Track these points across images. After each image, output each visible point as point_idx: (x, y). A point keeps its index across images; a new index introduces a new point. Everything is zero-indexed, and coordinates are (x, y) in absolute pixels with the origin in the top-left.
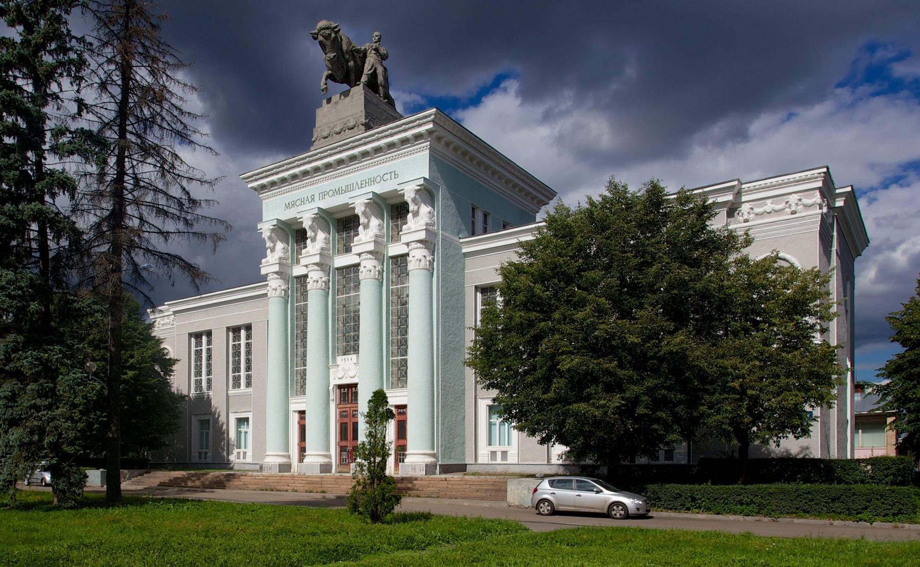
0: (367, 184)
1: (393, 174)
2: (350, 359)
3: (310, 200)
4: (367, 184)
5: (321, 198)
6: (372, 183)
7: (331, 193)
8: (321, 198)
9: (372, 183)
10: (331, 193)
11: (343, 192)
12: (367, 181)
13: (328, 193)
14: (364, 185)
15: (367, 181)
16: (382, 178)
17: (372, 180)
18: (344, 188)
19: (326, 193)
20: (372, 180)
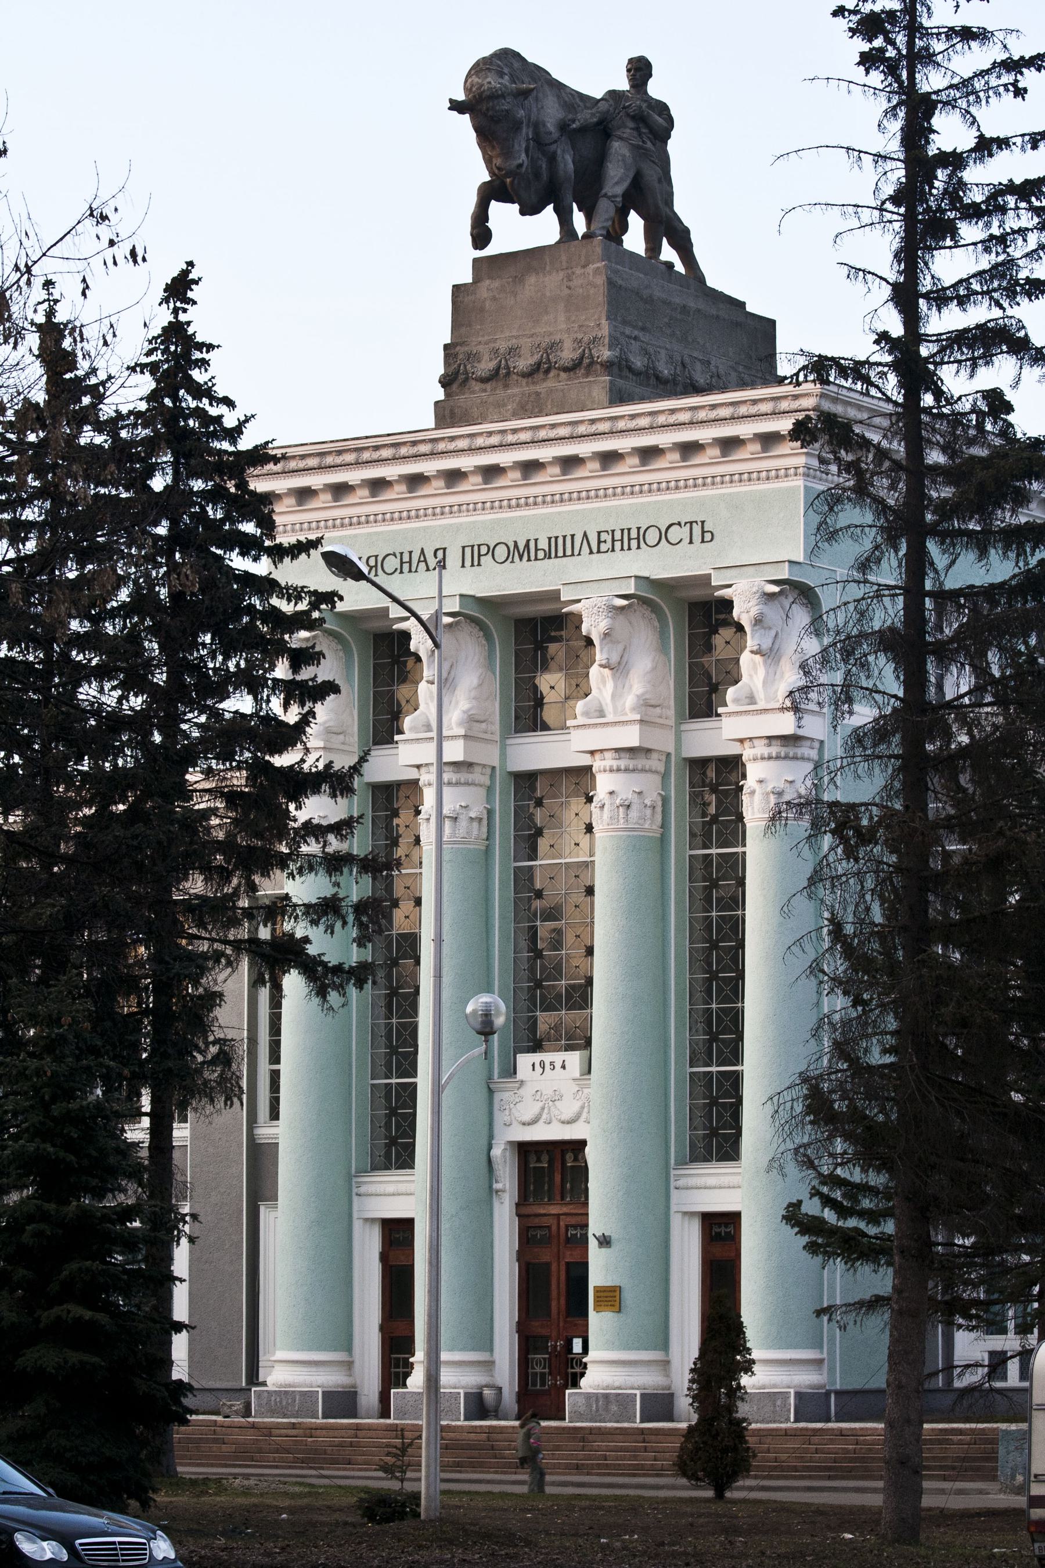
0: (618, 545)
1: (697, 530)
2: (537, 1066)
3: (432, 562)
4: (618, 545)
5: (468, 563)
6: (634, 543)
7: (501, 552)
8: (468, 563)
9: (634, 543)
10: (501, 552)
11: (541, 555)
12: (618, 536)
13: (491, 551)
14: (609, 545)
15: (618, 536)
16: (664, 535)
17: (634, 534)
18: (543, 544)
19: (484, 550)
20: (634, 534)
